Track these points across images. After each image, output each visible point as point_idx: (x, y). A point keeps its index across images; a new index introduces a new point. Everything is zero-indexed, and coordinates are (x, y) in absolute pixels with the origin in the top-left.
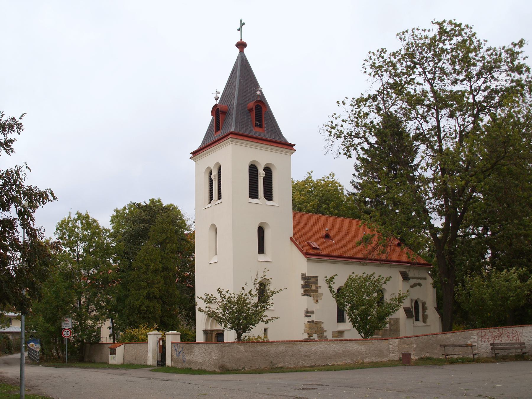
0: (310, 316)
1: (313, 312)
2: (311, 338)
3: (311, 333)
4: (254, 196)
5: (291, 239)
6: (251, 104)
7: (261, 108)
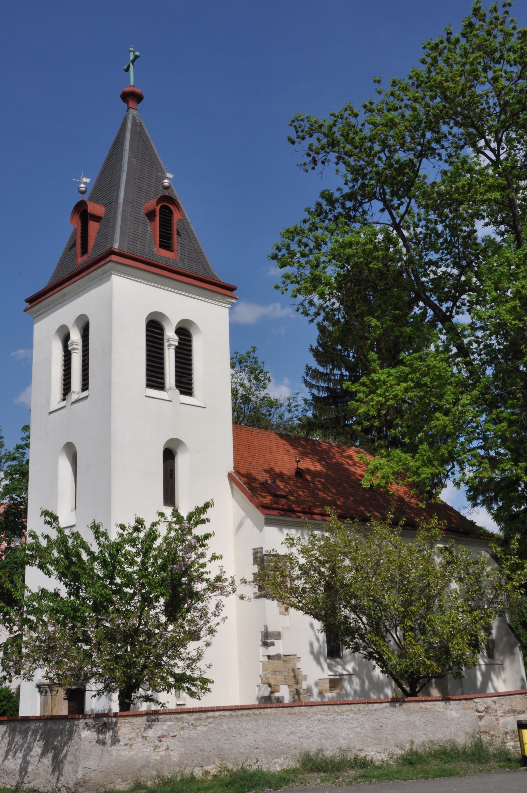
0: (273, 644)
1: (278, 636)
2: (277, 695)
3: (275, 683)
4: (156, 384)
5: (230, 476)
6: (151, 204)
7: (171, 212)
